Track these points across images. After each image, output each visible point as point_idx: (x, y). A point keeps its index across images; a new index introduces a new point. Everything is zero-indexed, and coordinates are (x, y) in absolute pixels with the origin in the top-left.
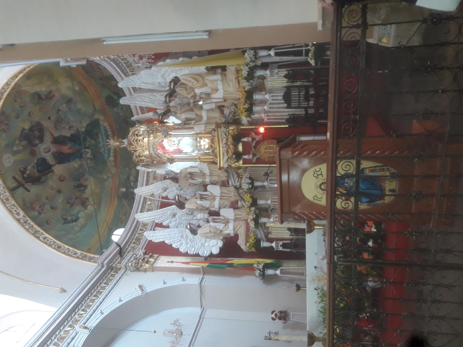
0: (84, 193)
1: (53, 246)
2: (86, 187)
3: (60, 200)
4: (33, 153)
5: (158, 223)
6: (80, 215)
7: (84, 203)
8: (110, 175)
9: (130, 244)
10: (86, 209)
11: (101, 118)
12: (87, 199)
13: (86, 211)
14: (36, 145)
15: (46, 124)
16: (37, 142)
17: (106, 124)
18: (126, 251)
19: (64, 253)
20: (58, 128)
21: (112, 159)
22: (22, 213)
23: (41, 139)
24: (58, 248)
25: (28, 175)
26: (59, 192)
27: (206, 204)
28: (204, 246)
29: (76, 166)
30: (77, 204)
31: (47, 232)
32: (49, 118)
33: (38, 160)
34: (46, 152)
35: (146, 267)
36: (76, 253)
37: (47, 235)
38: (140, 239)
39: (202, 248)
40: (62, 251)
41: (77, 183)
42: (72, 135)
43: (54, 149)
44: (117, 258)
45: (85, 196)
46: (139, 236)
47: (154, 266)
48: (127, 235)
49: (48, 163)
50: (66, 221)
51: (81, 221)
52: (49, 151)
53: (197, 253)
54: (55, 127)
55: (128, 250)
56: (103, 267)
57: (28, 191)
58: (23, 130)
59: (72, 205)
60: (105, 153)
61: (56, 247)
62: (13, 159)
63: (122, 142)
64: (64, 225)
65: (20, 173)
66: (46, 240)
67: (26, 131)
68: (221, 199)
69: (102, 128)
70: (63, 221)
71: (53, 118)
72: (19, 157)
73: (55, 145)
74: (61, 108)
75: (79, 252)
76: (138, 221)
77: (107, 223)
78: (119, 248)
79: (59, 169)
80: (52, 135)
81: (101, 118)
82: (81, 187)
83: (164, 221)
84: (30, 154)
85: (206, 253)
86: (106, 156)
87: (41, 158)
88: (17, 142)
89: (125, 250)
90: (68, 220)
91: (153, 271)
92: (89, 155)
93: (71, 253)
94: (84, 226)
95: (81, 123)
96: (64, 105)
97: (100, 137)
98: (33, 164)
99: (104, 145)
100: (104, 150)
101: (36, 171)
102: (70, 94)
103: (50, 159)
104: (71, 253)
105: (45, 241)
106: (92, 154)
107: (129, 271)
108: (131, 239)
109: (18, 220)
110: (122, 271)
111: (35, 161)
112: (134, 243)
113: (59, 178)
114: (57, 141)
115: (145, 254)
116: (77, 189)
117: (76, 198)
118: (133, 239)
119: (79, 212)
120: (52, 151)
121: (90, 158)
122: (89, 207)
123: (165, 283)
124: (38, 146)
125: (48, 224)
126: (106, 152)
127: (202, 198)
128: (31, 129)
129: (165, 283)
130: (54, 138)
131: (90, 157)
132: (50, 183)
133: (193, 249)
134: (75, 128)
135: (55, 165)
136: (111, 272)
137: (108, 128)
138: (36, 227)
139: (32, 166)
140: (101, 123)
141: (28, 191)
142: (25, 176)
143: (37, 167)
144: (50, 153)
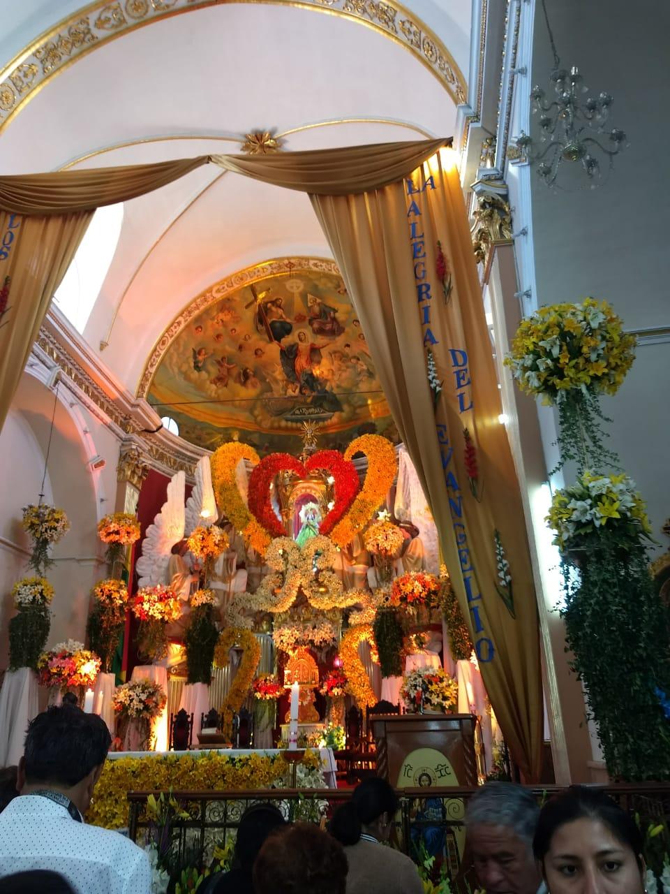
0: (235, 382)
1: (166, 335)
2: (244, 384)
3: (227, 348)
4: (300, 319)
5: (192, 490)
6: (204, 372)
7: (220, 380)
8: (259, 418)
9: (157, 445)
10: (211, 383)
11: (344, 415)
12: (226, 386)
13: (208, 382)
14: (311, 323)
15: (340, 340)
16: (316, 326)
18: (147, 439)
19: (155, 350)
20: (333, 356)
21: (283, 423)
22: (219, 296)
23: (320, 331)
24: (162, 342)
25: (270, 309)
26: (241, 348)
27: (219, 567)
28: (153, 564)
30: (219, 371)
31: (187, 327)
32: (348, 346)
33: (288, 323)
34: (299, 336)
35: (126, 471)
36: (152, 365)
37: (182, 326)
38: (163, 460)
39: (149, 562)
40: (158, 348)
41: (251, 373)
43: (304, 347)
44: (141, 426)
45: (231, 382)
46: (167, 458)
47: (127, 483)
48: (171, 441)
49: (283, 337)
50: (196, 353)
51: (195, 374)
52: (301, 340)
53: (143, 553)
54: (335, 352)
55: (147, 441)
56: (133, 406)
57: (247, 307)
58: (335, 311)
59: (218, 362)
60: (292, 415)
61: (164, 339)
62: (296, 291)
63: (312, 442)
64: (191, 349)
65: (274, 299)
66: (176, 325)
67: (332, 313)
68: (225, 592)
69: (327, 414)
70: (197, 350)
71: (347, 350)
72: (298, 300)
73: (309, 348)
74: (360, 362)
75: (153, 370)
76: (198, 460)
77: (187, 411)
78: (155, 429)
79: (273, 350)
80: (323, 347)
81: (344, 415)
83: (194, 500)
84: (300, 314)
85: (143, 567)
87: (291, 328)
88: (318, 301)
89: (148, 437)
90: (198, 356)
91: (118, 481)
92: (290, 392)
93: (154, 360)
94: (187, 377)
96: (365, 367)
98: (284, 316)
99: (304, 414)
100: (297, 414)
101: (274, 319)
103: (288, 340)
104: (154, 360)
105: (175, 323)
106: (292, 397)
107: (120, 445)
108: (168, 450)
109: (210, 290)
110: (123, 434)
111: (288, 320)
112: (157, 450)
113: (260, 350)
115: (144, 469)
116: (242, 371)
117: (229, 370)
118: (163, 449)
119: (208, 372)
120: (300, 343)
121: (286, 394)
122: (214, 387)
123: (102, 500)
124: (310, 327)
125: (196, 329)
126: (293, 416)
127: (228, 561)
128: (334, 320)
129: (102, 500)
130: (318, 349)
131: (288, 395)
132: (255, 337)
133: (150, 547)
134: (330, 377)
135: (280, 346)
136: (122, 417)
137: (329, 422)
138: (196, 312)
139: (281, 317)
140: (337, 414)
141: (247, 307)
142: (269, 305)
143: (281, 322)
144: (298, 341)
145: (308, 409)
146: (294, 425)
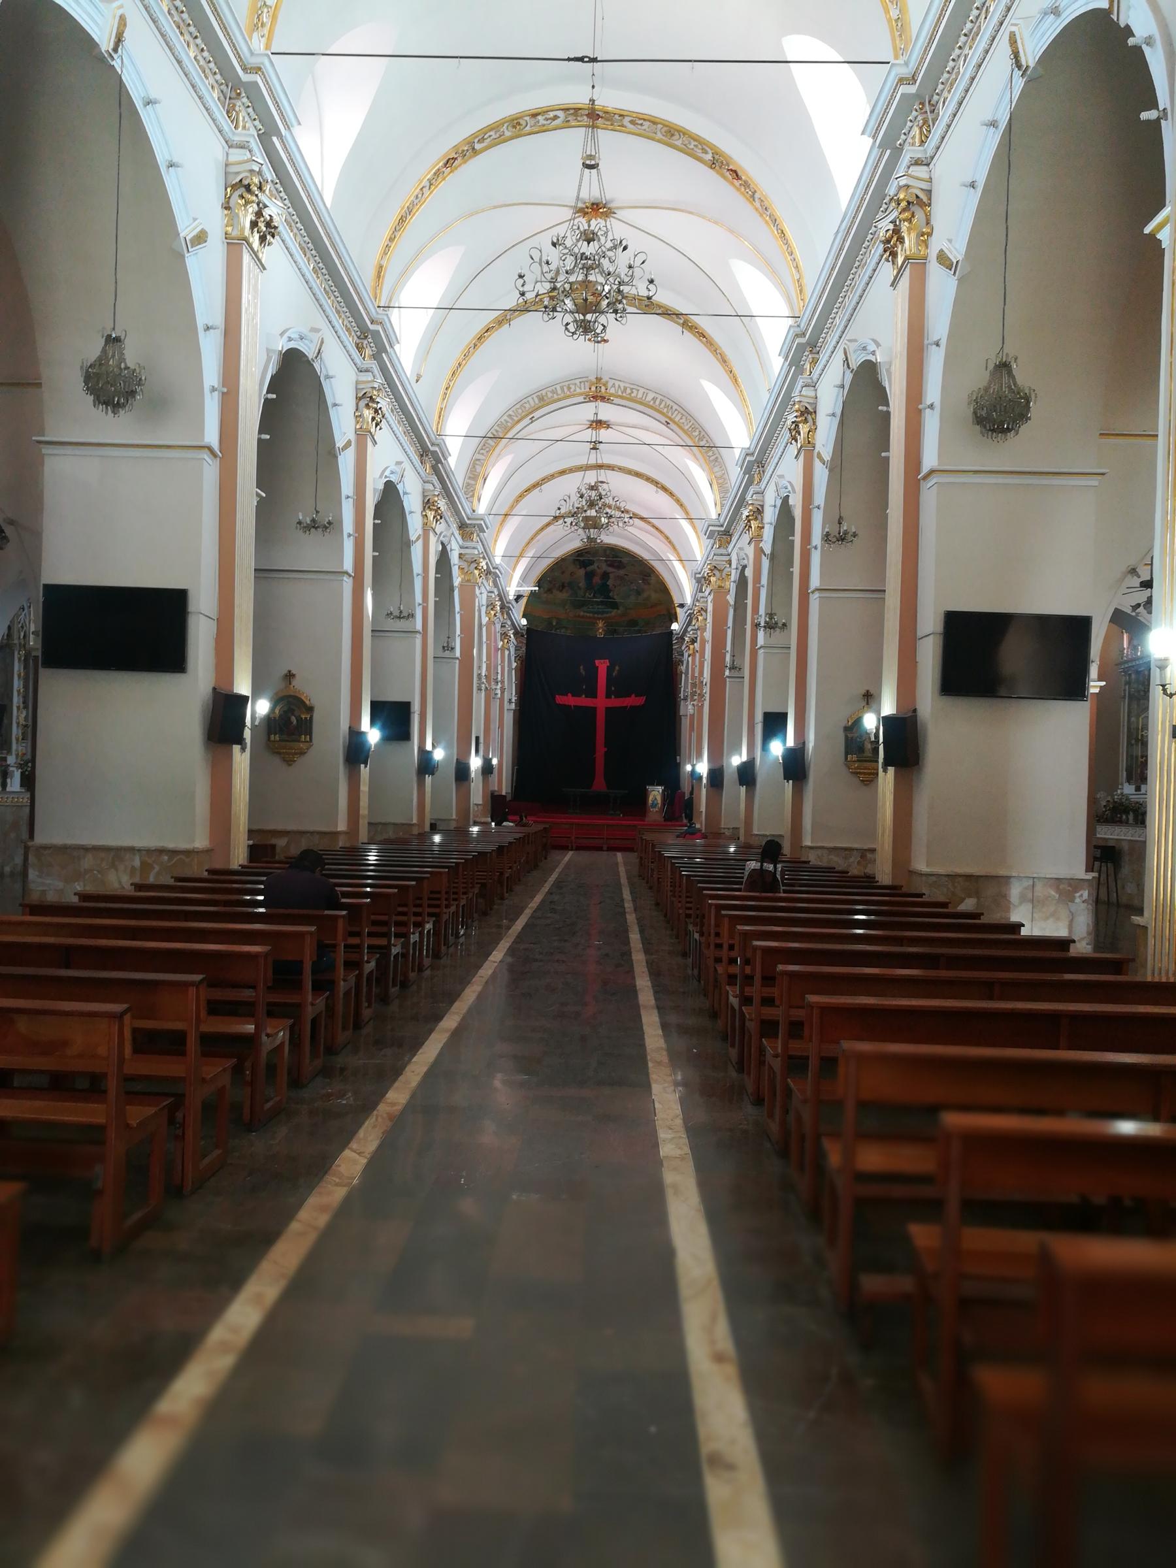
2: (561, 591)
8: (568, 610)
11: (619, 612)
15: (622, 572)
17: (613, 614)
21: (582, 614)
23: (611, 565)
26: (563, 573)
29: (580, 585)
42: (608, 586)
69: (610, 610)
74: (634, 584)
79: (582, 572)
80: (611, 573)
82: (562, 587)
86: (585, 608)
88: (613, 553)
95: (617, 595)
96: (635, 588)
97: (603, 607)
102: (645, 595)
103: (590, 568)
114: (605, 576)
122: (545, 595)
140: (615, 610)
145: (598, 605)
146: (588, 615)
